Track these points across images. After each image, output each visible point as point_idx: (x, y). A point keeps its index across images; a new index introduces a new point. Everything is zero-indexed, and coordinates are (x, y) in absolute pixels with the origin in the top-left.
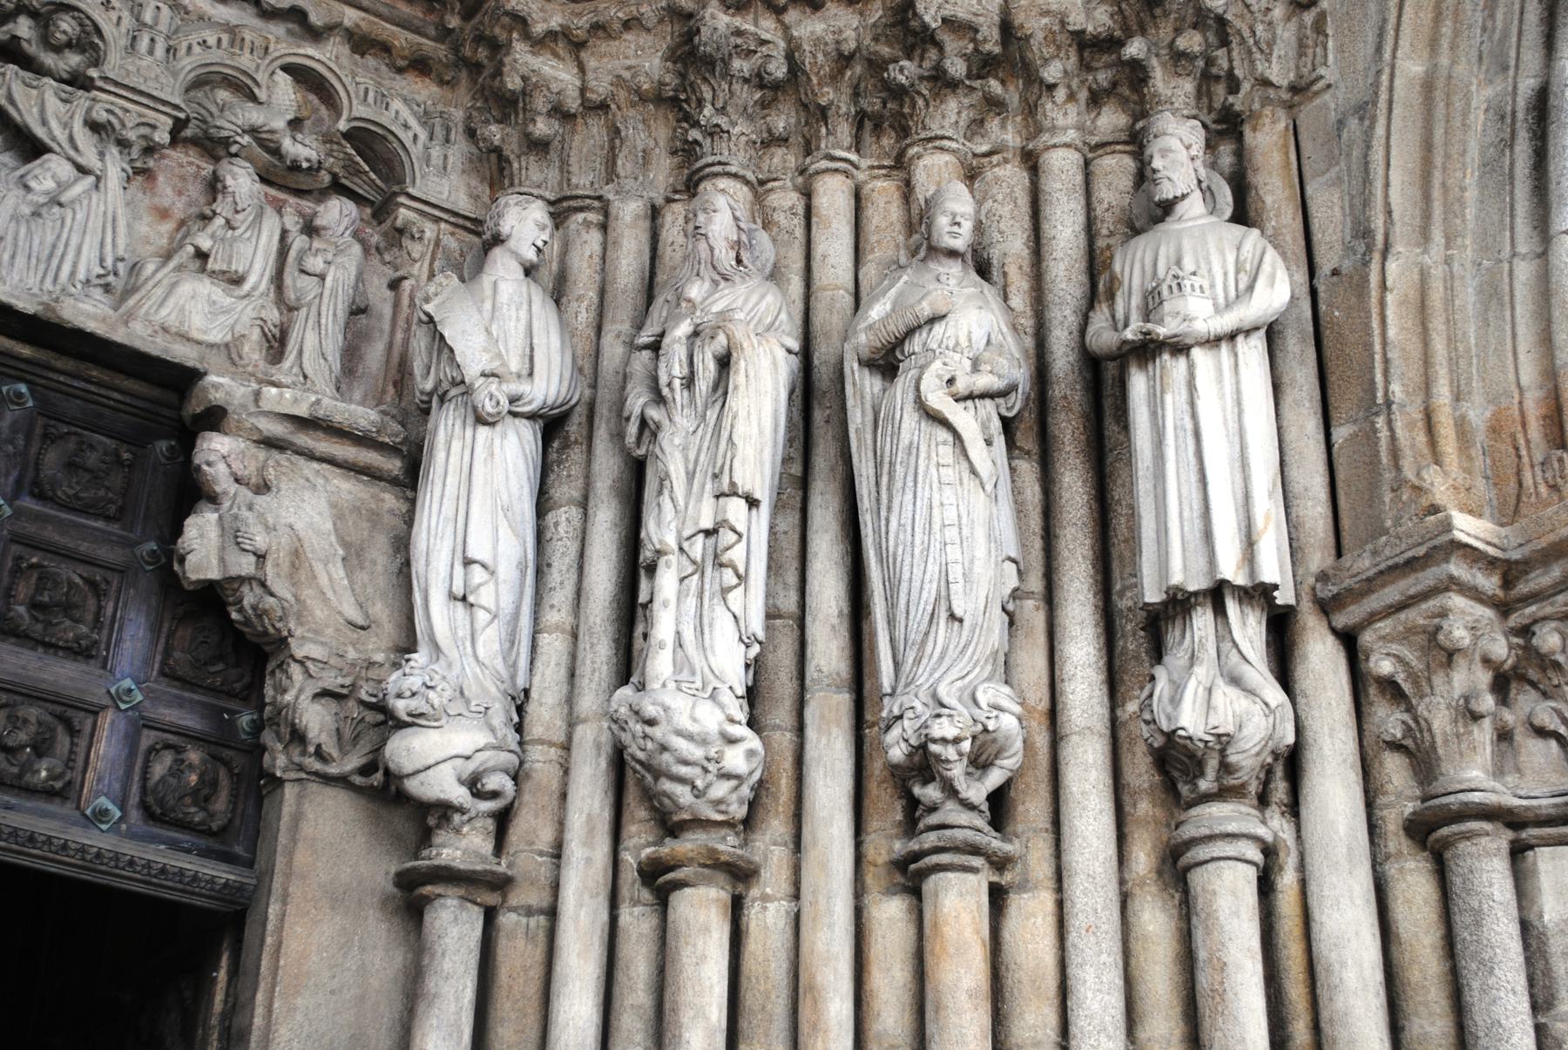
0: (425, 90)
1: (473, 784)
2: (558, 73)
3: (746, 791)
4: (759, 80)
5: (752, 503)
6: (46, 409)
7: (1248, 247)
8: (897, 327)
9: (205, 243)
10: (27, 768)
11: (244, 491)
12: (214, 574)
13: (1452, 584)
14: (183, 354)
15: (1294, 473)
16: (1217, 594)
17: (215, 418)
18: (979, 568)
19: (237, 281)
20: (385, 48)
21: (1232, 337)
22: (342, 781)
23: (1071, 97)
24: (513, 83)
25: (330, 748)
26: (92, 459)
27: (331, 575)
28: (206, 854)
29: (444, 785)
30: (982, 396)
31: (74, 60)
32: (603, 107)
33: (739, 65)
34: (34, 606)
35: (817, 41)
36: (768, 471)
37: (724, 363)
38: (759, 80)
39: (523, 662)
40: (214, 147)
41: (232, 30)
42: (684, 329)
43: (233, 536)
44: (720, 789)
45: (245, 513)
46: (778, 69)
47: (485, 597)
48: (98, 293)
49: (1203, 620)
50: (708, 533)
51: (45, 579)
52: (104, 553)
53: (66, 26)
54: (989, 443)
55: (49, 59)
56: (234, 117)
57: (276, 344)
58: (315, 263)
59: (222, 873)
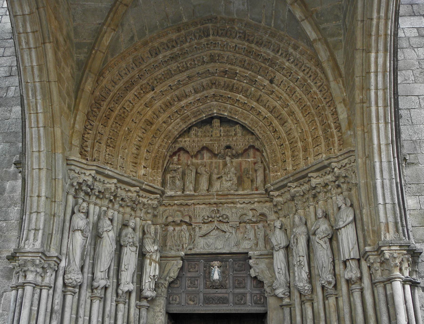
0: (268, 204)
1: (284, 294)
2: (280, 199)
3: (309, 291)
4: (300, 195)
5: (303, 256)
6: (234, 261)
7: (348, 212)
8: (313, 231)
9: (246, 236)
10: (241, 302)
11: (256, 265)
12: (254, 276)
13: (369, 255)
14: (246, 251)
15: (359, 240)
16: (348, 260)
17: (250, 258)
18: (326, 260)
19: (250, 239)
20: (261, 202)
21: (346, 225)
22: (273, 296)
23: (334, 189)
24: (275, 203)
25: (271, 292)
26: (240, 265)
27: (267, 272)
28: (262, 306)
29: (281, 295)
30: (325, 237)
31: (227, 219)
32: (286, 202)
33: (297, 194)
34: (238, 284)
35: (305, 189)
36: (305, 252)
37: (297, 239)
38: (300, 195)
39: (288, 278)
40: (245, 222)
41: (243, 208)
42: (292, 237)
43: (254, 270)
44: (306, 291)
45: (256, 268)
46: (302, 194)
47: (281, 272)
48: (235, 247)
49: (348, 263)
50: (299, 261)
51: (239, 281)
52: (244, 275)
53: (225, 216)
54: (326, 243)
55: (224, 221)
56: (246, 218)
57: (257, 244)
58: (259, 233)
59: (263, 309)
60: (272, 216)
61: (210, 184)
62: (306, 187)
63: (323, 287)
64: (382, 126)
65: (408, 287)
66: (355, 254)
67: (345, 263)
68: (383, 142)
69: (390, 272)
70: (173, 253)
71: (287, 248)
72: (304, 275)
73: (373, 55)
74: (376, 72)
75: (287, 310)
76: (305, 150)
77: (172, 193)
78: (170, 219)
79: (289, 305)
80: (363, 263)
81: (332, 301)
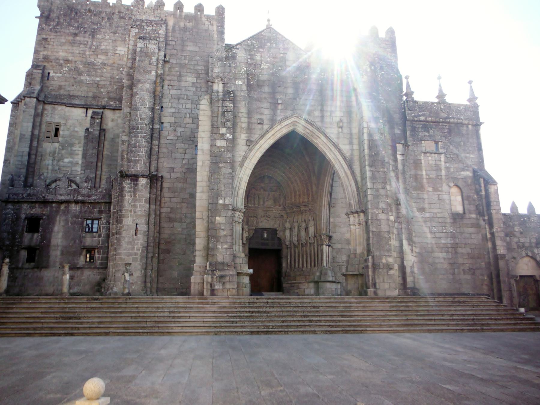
2: (289, 211)
17: (277, 231)
57: (279, 226)
60: (285, 217)
61: (264, 202)
62: (299, 209)
63: (302, 244)
64: (326, 199)
65: (327, 247)
66: (313, 235)
67: (310, 237)
68: (326, 203)
69: (323, 242)
70: (251, 228)
71: (290, 229)
72: (296, 239)
73: (327, 178)
74: (327, 183)
75: (289, 250)
76: (300, 196)
77: (250, 205)
78: (250, 215)
79: (290, 248)
80: (315, 238)
81: (304, 248)
